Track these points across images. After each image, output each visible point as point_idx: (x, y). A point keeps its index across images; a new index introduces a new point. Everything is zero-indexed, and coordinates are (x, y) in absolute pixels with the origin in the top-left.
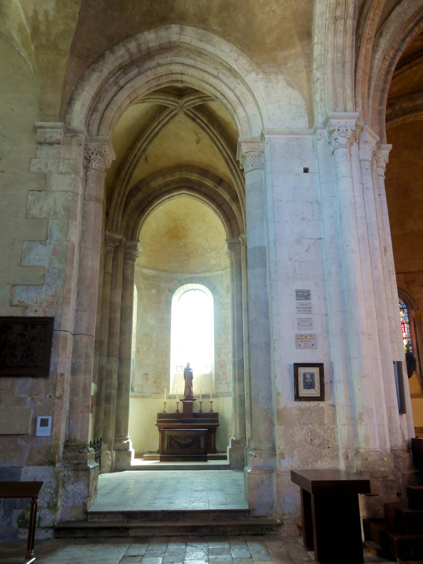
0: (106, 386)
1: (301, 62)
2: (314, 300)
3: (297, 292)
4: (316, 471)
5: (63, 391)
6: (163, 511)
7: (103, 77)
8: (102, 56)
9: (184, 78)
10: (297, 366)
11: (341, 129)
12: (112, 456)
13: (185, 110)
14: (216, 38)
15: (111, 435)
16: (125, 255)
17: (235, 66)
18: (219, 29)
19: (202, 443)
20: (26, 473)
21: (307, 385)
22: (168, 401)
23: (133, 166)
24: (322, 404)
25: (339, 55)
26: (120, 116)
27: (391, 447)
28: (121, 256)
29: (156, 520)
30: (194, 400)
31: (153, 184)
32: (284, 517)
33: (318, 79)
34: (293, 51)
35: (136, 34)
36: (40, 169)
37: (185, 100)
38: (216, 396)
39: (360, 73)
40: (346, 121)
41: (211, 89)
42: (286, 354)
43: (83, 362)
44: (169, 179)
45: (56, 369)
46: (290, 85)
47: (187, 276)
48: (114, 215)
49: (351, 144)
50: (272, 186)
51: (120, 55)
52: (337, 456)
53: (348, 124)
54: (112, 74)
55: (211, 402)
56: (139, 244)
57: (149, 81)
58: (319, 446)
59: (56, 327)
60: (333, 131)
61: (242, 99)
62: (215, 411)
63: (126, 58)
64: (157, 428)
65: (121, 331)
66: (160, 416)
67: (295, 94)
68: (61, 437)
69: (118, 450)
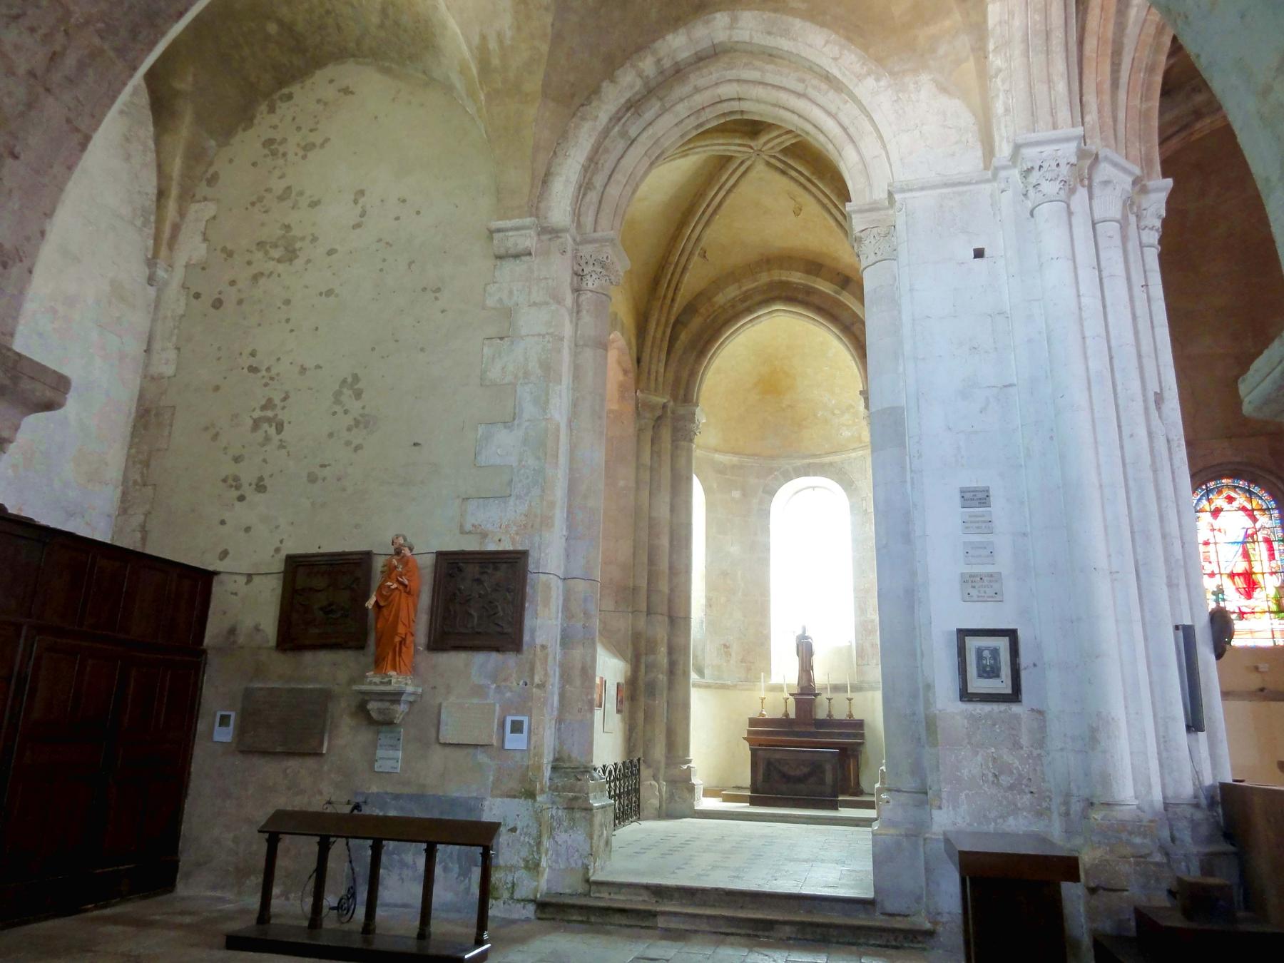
0: (646, 666)
1: (964, 42)
2: (999, 507)
3: (963, 491)
4: (1004, 835)
5: (546, 674)
6: (717, 889)
7: (600, 129)
8: (595, 92)
9: (745, 106)
10: (963, 634)
11: (1045, 165)
12: (660, 790)
13: (767, 158)
14: (798, 23)
15: (659, 752)
16: (675, 430)
17: (835, 71)
18: (803, 6)
19: (829, 777)
20: (491, 809)
21: (985, 671)
22: (770, 697)
23: (679, 270)
24: (1015, 708)
25: (1037, 17)
26: (634, 192)
27: (1165, 798)
28: (666, 434)
29: (704, 904)
30: (816, 695)
31: (720, 299)
32: (939, 918)
33: (1000, 70)
34: (947, 23)
35: (654, 41)
36: (501, 300)
37: (763, 139)
38: (857, 688)
39: (1091, 44)
40: (1056, 147)
41: (795, 118)
42: (949, 611)
43: (579, 625)
44: (748, 285)
45: (533, 638)
46: (943, 90)
47: (799, 463)
48: (650, 362)
49: (1072, 191)
50: (911, 290)
51: (628, 82)
52: (1048, 809)
53: (1060, 153)
54: (616, 118)
55: (850, 700)
56: (698, 410)
57: (682, 121)
58: (1011, 788)
59: (531, 567)
60: (1030, 170)
61: (852, 130)
62: (857, 716)
63: (637, 88)
64: (747, 744)
65: (671, 568)
66: (753, 722)
67: (954, 105)
68: (546, 752)
69: (672, 782)
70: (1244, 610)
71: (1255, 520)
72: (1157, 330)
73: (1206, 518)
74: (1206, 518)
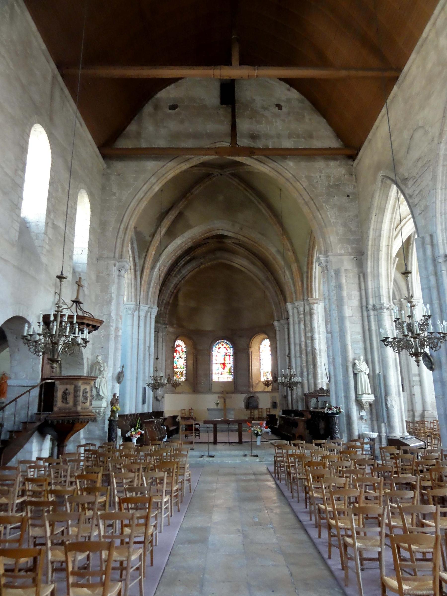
39: (143, 282)
71: (227, 350)
73: (217, 349)
74: (217, 349)
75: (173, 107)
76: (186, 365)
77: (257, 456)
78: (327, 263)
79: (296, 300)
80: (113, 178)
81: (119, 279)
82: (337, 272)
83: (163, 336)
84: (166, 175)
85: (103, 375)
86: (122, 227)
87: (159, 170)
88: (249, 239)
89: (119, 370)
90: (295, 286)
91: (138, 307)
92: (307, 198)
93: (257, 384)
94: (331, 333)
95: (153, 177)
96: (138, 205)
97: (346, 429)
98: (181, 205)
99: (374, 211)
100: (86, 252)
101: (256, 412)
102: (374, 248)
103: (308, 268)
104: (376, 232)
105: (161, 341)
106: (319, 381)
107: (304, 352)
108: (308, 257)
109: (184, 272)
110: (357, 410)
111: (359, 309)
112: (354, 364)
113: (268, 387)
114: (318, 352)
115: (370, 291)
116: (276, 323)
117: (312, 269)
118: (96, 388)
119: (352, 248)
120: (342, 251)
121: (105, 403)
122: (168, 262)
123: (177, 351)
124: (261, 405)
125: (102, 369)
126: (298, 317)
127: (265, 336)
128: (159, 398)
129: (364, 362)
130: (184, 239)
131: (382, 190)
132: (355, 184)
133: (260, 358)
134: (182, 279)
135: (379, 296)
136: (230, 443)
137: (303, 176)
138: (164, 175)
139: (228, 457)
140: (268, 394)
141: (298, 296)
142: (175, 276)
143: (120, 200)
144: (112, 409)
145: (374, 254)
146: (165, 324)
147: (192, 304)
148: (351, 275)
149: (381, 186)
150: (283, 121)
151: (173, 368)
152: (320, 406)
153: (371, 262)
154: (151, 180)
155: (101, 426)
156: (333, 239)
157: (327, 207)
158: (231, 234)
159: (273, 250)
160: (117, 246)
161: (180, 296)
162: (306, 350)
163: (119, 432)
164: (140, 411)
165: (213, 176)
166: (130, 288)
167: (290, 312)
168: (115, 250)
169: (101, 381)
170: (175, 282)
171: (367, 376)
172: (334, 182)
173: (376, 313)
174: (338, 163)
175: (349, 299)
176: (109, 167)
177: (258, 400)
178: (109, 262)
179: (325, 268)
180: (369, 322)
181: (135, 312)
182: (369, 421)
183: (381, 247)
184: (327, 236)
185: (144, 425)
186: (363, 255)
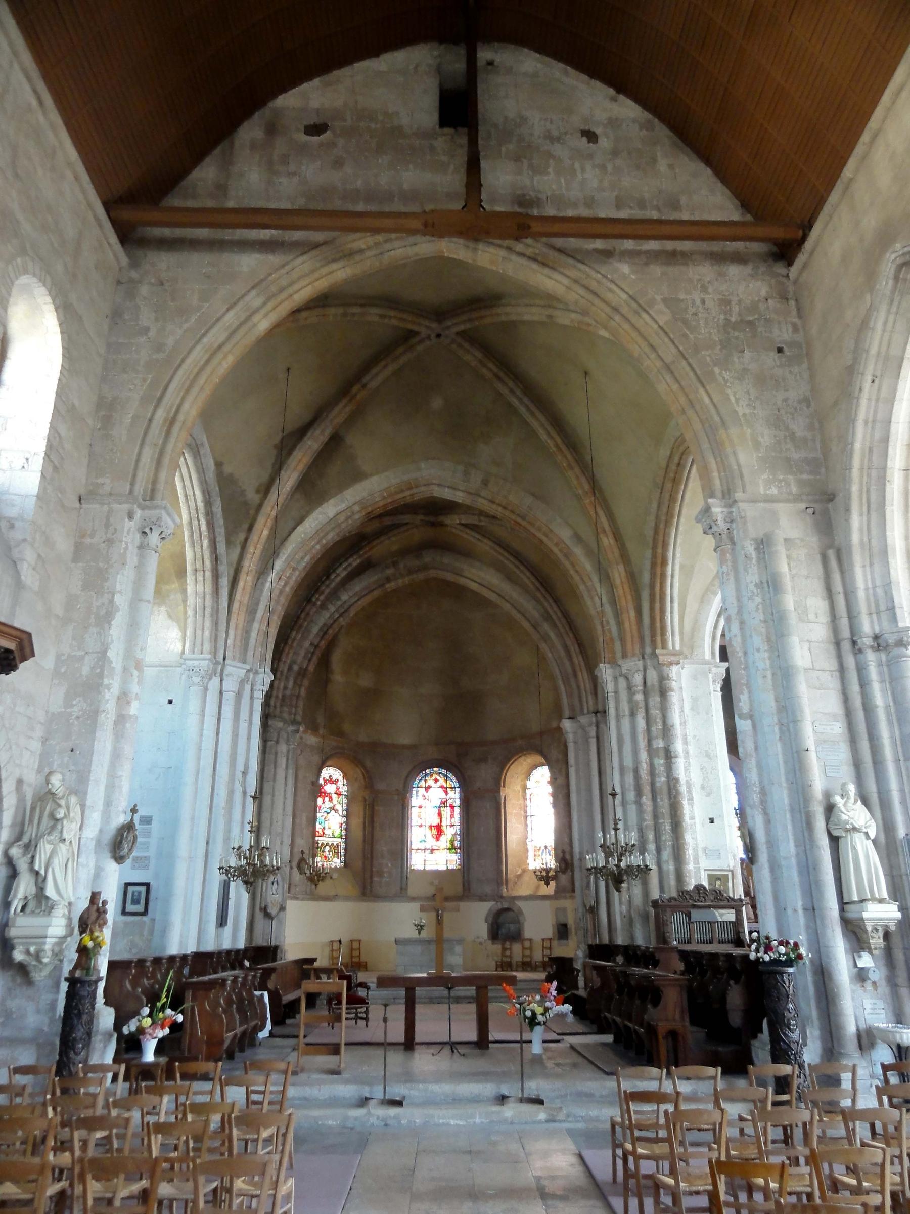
1: (179, 596)
10: (127, 885)
24: (145, 918)
34: (173, 586)
39: (236, 605)
46: (170, 617)
70: (434, 847)
71: (446, 793)
72: (252, 740)
73: (422, 791)
74: (422, 791)
75: (316, 129)
76: (346, 829)
77: (540, 1102)
78: (732, 522)
79: (624, 656)
80: (144, 290)
81: (142, 557)
82: (764, 545)
83: (288, 751)
84: (290, 290)
85: (61, 832)
86: (161, 414)
87: (270, 274)
88: (505, 508)
89: (121, 819)
90: (620, 624)
91: (218, 668)
92: (669, 353)
93: (519, 877)
94: (751, 717)
95: (253, 293)
96: (208, 361)
97: (814, 1014)
98: (338, 415)
99: (869, 369)
100: (38, 463)
101: (517, 949)
102: (869, 475)
103: (653, 575)
104: (873, 428)
105: (284, 766)
106: (691, 866)
107: (647, 789)
108: (654, 548)
109: (344, 597)
110: (846, 952)
111: (832, 648)
112: (830, 809)
113: (547, 884)
114: (683, 789)
115: (861, 594)
116: (567, 725)
117: (663, 576)
118: (37, 873)
119: (801, 483)
120: (774, 491)
121: (63, 922)
122: (302, 558)
123: (325, 793)
124: (527, 934)
125: (60, 814)
126: (631, 700)
127: (540, 759)
128: (273, 911)
129: (859, 802)
130: (343, 506)
131: (895, 303)
132: (796, 320)
133: (526, 812)
134: (341, 615)
135: (893, 608)
136: (453, 1046)
137: (658, 298)
138: (282, 290)
139: (444, 1104)
140: (547, 903)
141: (629, 646)
142: (323, 606)
143: (159, 348)
144: (81, 940)
145: (868, 491)
146: (294, 722)
147: (366, 681)
148: (801, 553)
149: (893, 291)
150: (603, 168)
151: (314, 836)
152: (696, 937)
153: (861, 515)
154: (247, 299)
155: (46, 998)
156: (745, 458)
157: (726, 375)
158: (459, 497)
159: (565, 534)
160: (141, 465)
161: (336, 658)
162: (653, 784)
163: (106, 1017)
164: (210, 946)
165: (417, 339)
166: (199, 619)
167: (610, 687)
168: (134, 476)
169: (53, 853)
170: (321, 624)
171: (870, 844)
172: (740, 314)
173: (883, 656)
174: (748, 269)
175: (801, 620)
176: (134, 264)
177: (521, 918)
178: (115, 506)
179: (724, 536)
180: (864, 684)
181: (210, 679)
182: (883, 988)
183: (888, 472)
184: (729, 450)
185: (189, 994)
186: (831, 500)
